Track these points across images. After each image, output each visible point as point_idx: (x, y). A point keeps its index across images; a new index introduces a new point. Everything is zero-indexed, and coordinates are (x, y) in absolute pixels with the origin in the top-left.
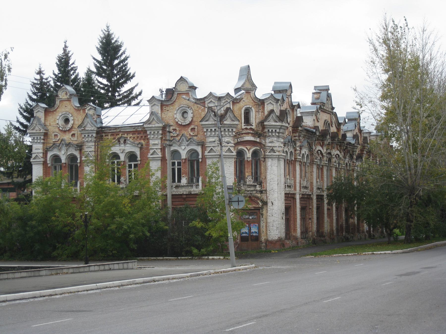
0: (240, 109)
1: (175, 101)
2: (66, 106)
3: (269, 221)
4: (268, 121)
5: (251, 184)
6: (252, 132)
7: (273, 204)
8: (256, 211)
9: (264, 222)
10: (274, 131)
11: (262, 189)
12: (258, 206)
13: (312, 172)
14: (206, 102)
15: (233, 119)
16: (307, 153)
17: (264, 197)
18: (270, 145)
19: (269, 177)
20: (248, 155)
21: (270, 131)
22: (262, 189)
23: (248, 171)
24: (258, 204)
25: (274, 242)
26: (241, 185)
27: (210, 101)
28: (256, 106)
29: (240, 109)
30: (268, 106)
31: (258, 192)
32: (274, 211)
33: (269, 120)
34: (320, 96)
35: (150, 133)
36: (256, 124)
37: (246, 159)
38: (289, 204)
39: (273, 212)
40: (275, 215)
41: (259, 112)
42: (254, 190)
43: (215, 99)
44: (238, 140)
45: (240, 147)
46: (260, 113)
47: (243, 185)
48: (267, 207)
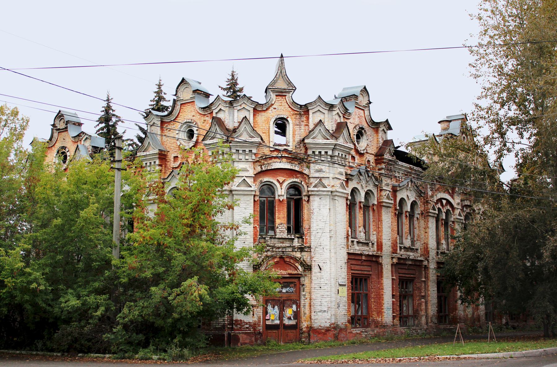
0: (268, 121)
1: (178, 115)
2: (64, 139)
3: (313, 297)
4: (312, 137)
5: (284, 237)
6: (287, 155)
7: (320, 269)
8: (293, 280)
9: (306, 299)
10: (323, 153)
11: (303, 245)
12: (296, 272)
13: (426, 228)
14: (215, 112)
15: (251, 134)
16: (412, 199)
17: (305, 256)
18: (317, 175)
19: (314, 226)
20: (281, 192)
21: (317, 153)
22: (303, 245)
23: (280, 216)
24: (296, 268)
25: (323, 331)
26: (266, 238)
27: (218, 109)
28: (295, 116)
29: (268, 121)
30: (315, 115)
31: (296, 250)
32: (322, 280)
33: (314, 136)
34: (448, 126)
35: (146, 164)
36: (295, 143)
37: (277, 198)
38: (369, 271)
39: (321, 282)
40: (326, 288)
41: (300, 125)
42: (290, 247)
43: (225, 106)
44: (262, 168)
45: (266, 179)
46: (303, 127)
47: (270, 238)
48: (311, 274)
